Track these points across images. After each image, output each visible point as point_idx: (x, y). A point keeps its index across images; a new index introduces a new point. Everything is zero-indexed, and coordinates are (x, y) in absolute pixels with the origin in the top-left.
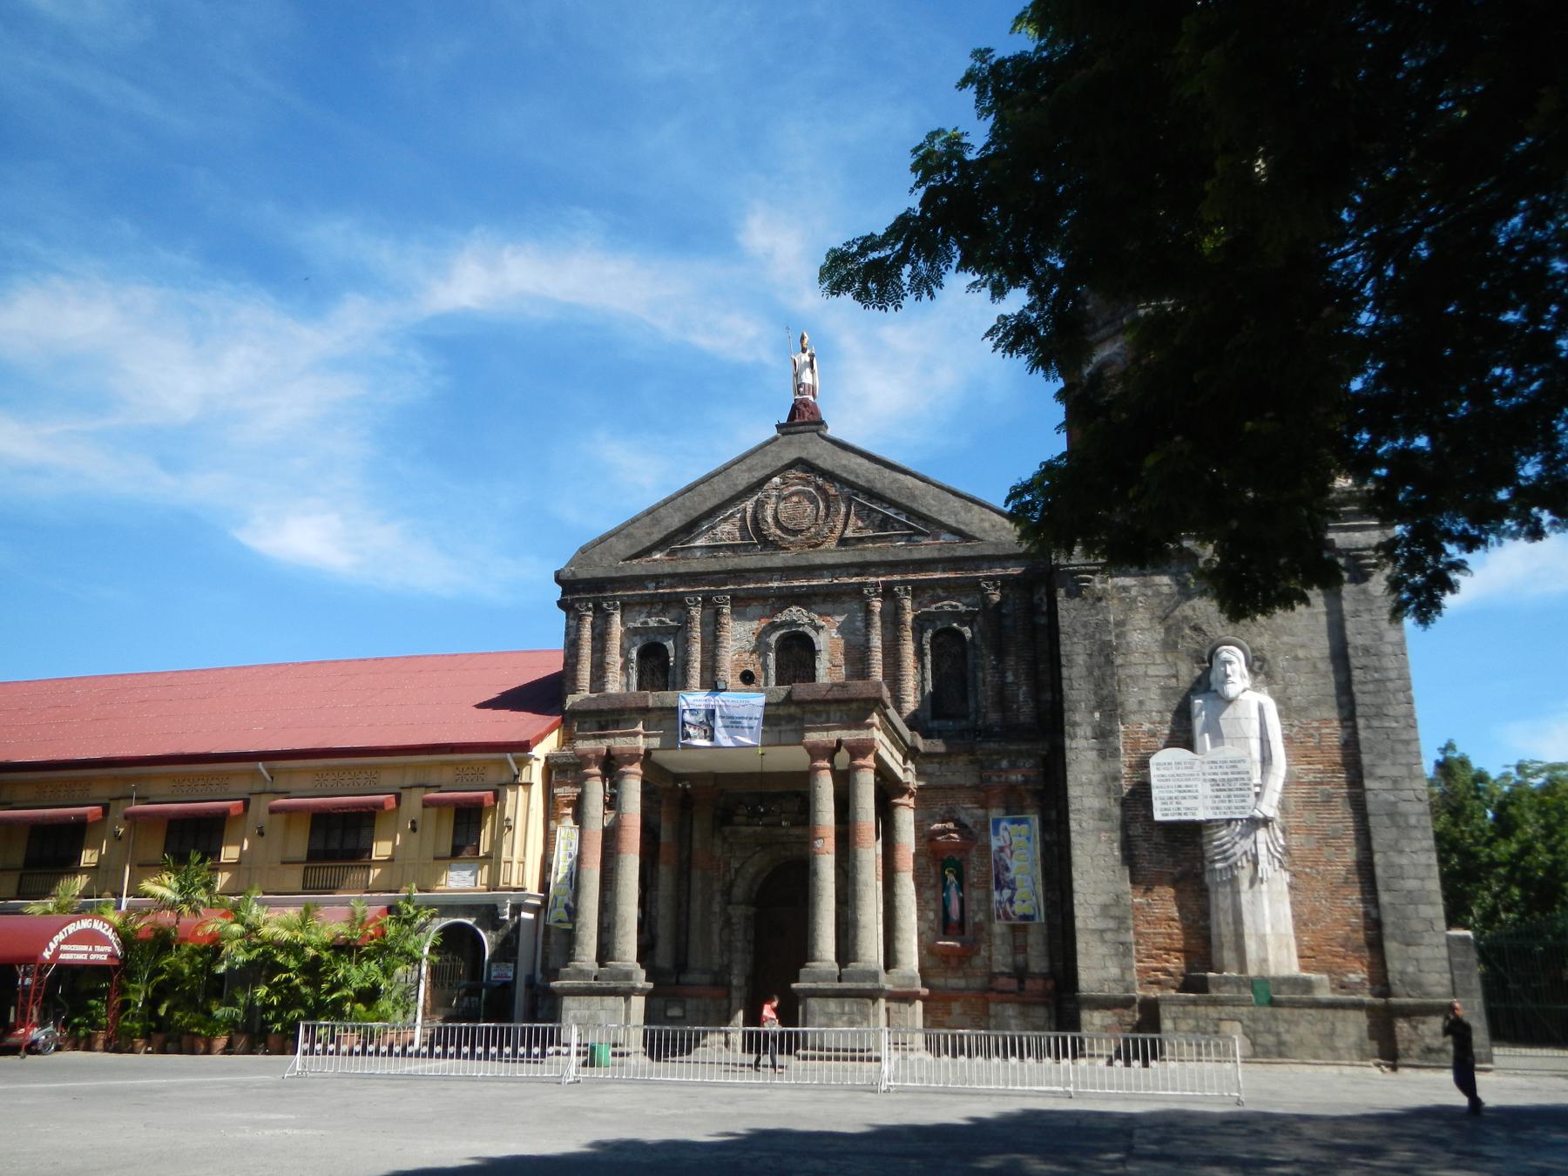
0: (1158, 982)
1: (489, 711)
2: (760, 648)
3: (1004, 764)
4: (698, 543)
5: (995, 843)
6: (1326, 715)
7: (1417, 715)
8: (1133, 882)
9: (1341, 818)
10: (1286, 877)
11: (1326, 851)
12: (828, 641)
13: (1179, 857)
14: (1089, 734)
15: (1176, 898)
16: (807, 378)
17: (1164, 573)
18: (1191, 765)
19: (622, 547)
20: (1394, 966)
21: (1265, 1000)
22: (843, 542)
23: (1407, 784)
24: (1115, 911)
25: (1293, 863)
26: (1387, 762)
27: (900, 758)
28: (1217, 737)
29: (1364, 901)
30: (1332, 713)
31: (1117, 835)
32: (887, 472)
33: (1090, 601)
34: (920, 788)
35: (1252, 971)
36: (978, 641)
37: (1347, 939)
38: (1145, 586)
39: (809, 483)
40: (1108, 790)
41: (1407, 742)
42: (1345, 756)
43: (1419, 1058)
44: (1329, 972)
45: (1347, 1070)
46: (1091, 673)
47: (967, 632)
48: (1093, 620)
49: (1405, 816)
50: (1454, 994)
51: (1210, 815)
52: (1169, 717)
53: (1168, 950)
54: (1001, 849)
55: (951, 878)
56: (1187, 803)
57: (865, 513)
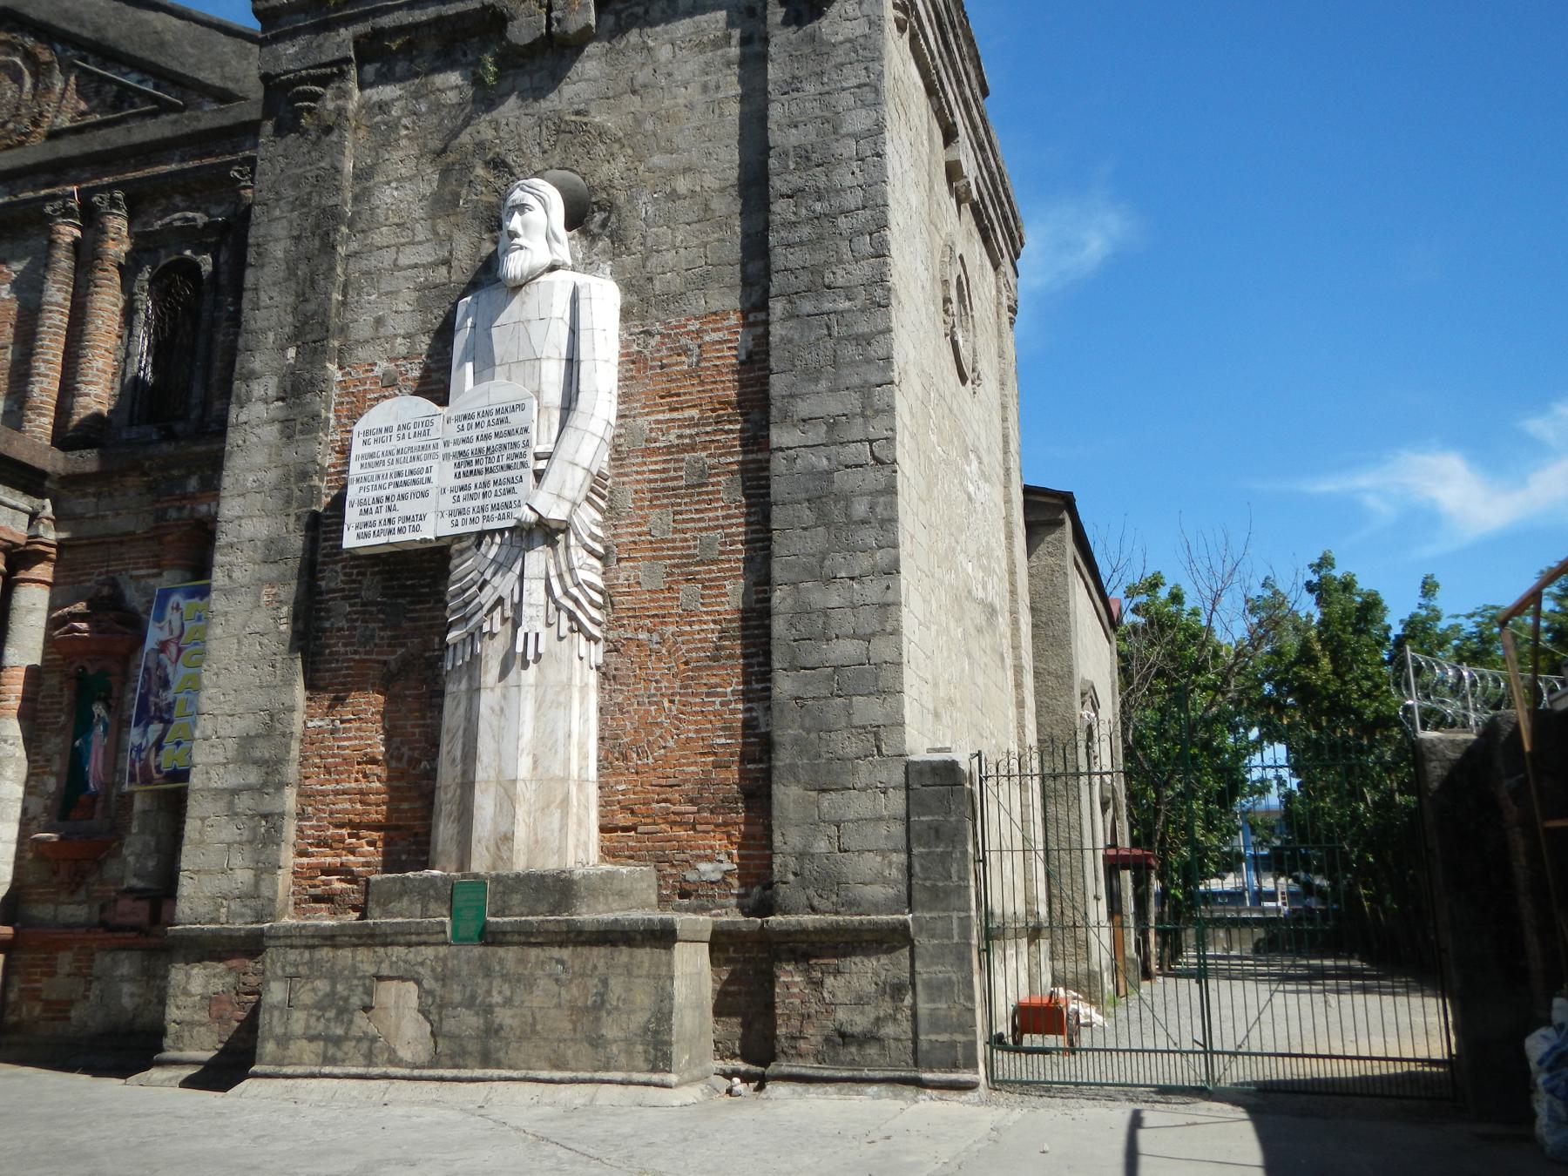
0: (327, 898)
3: (193, 483)
5: (154, 635)
6: (715, 305)
7: (894, 280)
8: (310, 686)
9: (724, 513)
10: (596, 654)
11: (685, 591)
13: (392, 624)
14: (272, 392)
17: (451, 66)
20: (787, 839)
21: (474, 929)
22: (54, 135)
23: (856, 431)
24: (263, 750)
25: (616, 624)
26: (823, 385)
28: (485, 363)
29: (746, 696)
30: (732, 301)
31: (289, 591)
33: (313, 137)
34: (60, 545)
35: (480, 863)
36: (223, 279)
37: (704, 783)
38: (417, 95)
40: (288, 501)
41: (865, 340)
43: (819, 1057)
45: (608, 1095)
46: (292, 272)
47: (206, 263)
49: (847, 498)
50: (910, 904)
51: (446, 529)
52: (424, 343)
53: (356, 827)
54: (163, 646)
55: (99, 709)
56: (405, 508)
57: (89, 87)
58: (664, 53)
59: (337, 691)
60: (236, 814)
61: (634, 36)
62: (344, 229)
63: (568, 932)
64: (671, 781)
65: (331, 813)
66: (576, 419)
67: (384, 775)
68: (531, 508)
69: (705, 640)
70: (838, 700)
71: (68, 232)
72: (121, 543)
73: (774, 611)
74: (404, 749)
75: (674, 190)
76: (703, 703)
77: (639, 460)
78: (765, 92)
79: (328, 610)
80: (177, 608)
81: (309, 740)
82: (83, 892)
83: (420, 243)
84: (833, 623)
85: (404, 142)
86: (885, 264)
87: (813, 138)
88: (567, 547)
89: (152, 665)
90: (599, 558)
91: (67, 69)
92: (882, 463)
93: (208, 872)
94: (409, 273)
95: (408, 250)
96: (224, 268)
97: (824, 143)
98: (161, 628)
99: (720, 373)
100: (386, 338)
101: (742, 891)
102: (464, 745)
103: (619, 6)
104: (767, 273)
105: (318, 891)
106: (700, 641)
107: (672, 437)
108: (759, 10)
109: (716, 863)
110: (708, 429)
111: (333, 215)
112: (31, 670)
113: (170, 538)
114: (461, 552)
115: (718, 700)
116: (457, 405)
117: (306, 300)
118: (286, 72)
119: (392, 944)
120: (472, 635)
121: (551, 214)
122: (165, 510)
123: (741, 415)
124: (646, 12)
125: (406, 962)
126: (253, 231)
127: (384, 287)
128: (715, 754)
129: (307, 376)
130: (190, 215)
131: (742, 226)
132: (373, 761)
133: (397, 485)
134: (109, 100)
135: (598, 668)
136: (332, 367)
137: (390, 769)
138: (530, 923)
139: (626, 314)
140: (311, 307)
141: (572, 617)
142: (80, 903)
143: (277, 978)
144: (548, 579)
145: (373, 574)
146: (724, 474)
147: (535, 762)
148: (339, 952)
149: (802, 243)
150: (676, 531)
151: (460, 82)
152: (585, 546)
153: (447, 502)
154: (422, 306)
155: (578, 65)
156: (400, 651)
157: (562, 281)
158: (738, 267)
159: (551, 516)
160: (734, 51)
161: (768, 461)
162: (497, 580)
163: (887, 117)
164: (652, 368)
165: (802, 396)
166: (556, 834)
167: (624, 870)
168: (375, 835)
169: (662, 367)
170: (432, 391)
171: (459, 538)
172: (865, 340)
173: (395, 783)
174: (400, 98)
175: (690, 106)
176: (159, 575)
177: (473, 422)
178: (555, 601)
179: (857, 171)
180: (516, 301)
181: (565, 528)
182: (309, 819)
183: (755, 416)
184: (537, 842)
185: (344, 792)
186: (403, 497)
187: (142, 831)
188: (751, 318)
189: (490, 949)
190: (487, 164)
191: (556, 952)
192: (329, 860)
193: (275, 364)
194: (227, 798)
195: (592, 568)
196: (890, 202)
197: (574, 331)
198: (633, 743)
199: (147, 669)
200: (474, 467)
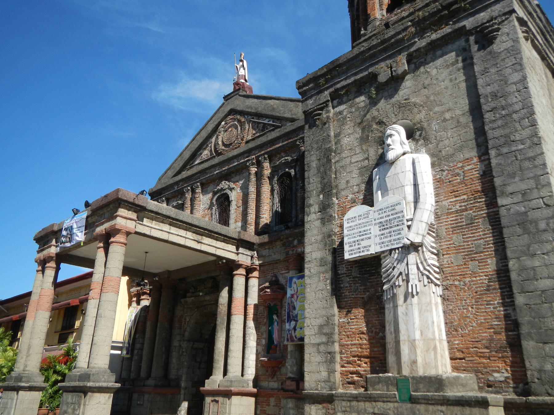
0: (352, 383)
1: (110, 255)
2: (210, 208)
3: (296, 242)
4: (196, 163)
5: (289, 292)
6: (467, 156)
7: (541, 134)
8: (339, 307)
9: (483, 234)
12: (235, 196)
13: (364, 284)
14: (317, 210)
15: (365, 316)
16: (242, 72)
17: (361, 95)
18: (368, 213)
19: (170, 173)
20: (532, 364)
21: (407, 397)
22: (247, 142)
23: (535, 194)
24: (326, 330)
25: (445, 279)
26: (517, 179)
27: (233, 248)
28: (385, 190)
29: (504, 304)
30: (473, 154)
31: (329, 275)
32: (264, 102)
33: (320, 127)
34: (260, 265)
35: (406, 372)
36: (298, 176)
37: (491, 340)
38: (351, 107)
39: (235, 120)
40: (325, 245)
41: (533, 158)
42: (483, 183)
44: (477, 372)
46: (319, 171)
47: (292, 172)
48: (321, 138)
49: (535, 222)
52: (363, 187)
53: (360, 357)
54: (292, 296)
55: (275, 317)
56: (364, 243)
57: (255, 126)
58: (434, 72)
59: (348, 309)
60: (320, 352)
61: (422, 69)
62: (333, 154)
63: (443, 400)
64: (477, 340)
65: (351, 352)
66: (420, 205)
67: (367, 338)
68: (408, 239)
69: (483, 283)
70: (546, 305)
71: (253, 170)
72: (277, 263)
73: (511, 270)
74: (373, 329)
75: (445, 118)
76: (486, 308)
77: (446, 217)
78: (475, 76)
79: (342, 281)
80: (295, 283)
81: (341, 326)
82: (275, 379)
83: (358, 154)
84: (538, 273)
85: (349, 122)
86: (537, 128)
87: (497, 88)
88: (423, 252)
89: (290, 302)
90: (435, 255)
91: (249, 122)
92: (549, 206)
93: (313, 372)
94: (355, 164)
95: (354, 157)
96: (298, 173)
97: (502, 88)
98: (291, 290)
99: (473, 181)
100: (350, 187)
101: (515, 385)
102: (394, 327)
103: (415, 61)
104: (486, 141)
105: (349, 380)
106: (480, 283)
107: (457, 207)
108: (467, 48)
109: (502, 373)
110: (472, 202)
111: (329, 150)
112: (255, 305)
113: (290, 260)
114: (385, 257)
115: (492, 307)
116: (377, 206)
117: (324, 179)
118: (310, 109)
119: (378, 401)
120: (392, 286)
121: (401, 136)
122: (288, 251)
123: (484, 195)
124: (425, 60)
125: (383, 408)
126: (306, 160)
127: (348, 170)
128: (494, 328)
129: (327, 203)
130: (286, 158)
131: (473, 126)
132: (363, 333)
133: (360, 236)
134: (261, 129)
135: (441, 296)
136: (334, 199)
137: (369, 336)
138: (428, 395)
139: (433, 165)
140: (326, 181)
141: (428, 277)
142: (275, 382)
143: (339, 412)
144: (417, 264)
145: (356, 267)
146: (480, 218)
147: (421, 333)
148: (360, 403)
149: (499, 127)
150: (464, 242)
151: (364, 99)
152: (429, 251)
153: (378, 240)
154: (361, 174)
155: (404, 84)
156: (368, 293)
157: (408, 158)
158: (474, 141)
159: (416, 241)
160: (460, 65)
161: (498, 211)
162: (399, 266)
163: (527, 73)
164: (446, 183)
165: (509, 184)
166: (433, 361)
167: (463, 375)
168: (367, 360)
169: (450, 182)
170: (368, 202)
171: (383, 252)
172: (533, 158)
173: (371, 341)
174: (346, 108)
175: (446, 88)
176: (289, 272)
177: (383, 211)
178: (421, 272)
179: (518, 96)
180: (393, 167)
181: (421, 245)
182: (344, 354)
183: (490, 195)
184: (426, 363)
185: (354, 344)
186: (362, 240)
187: (291, 358)
188: (482, 158)
189: (414, 405)
190: (377, 123)
191: (440, 408)
192: (352, 369)
193: (317, 201)
194: (317, 346)
195: (433, 259)
196: (534, 104)
197: (415, 174)
198: (459, 324)
199: (288, 303)
200: (385, 227)
